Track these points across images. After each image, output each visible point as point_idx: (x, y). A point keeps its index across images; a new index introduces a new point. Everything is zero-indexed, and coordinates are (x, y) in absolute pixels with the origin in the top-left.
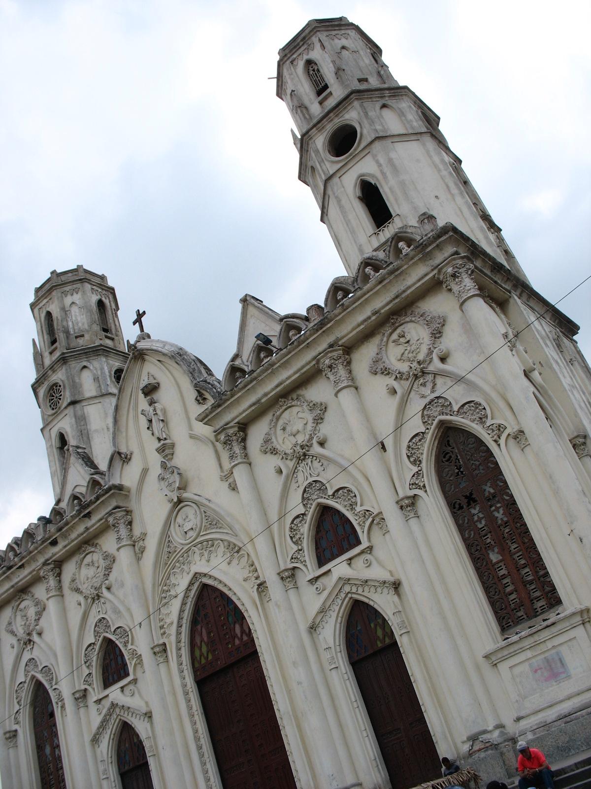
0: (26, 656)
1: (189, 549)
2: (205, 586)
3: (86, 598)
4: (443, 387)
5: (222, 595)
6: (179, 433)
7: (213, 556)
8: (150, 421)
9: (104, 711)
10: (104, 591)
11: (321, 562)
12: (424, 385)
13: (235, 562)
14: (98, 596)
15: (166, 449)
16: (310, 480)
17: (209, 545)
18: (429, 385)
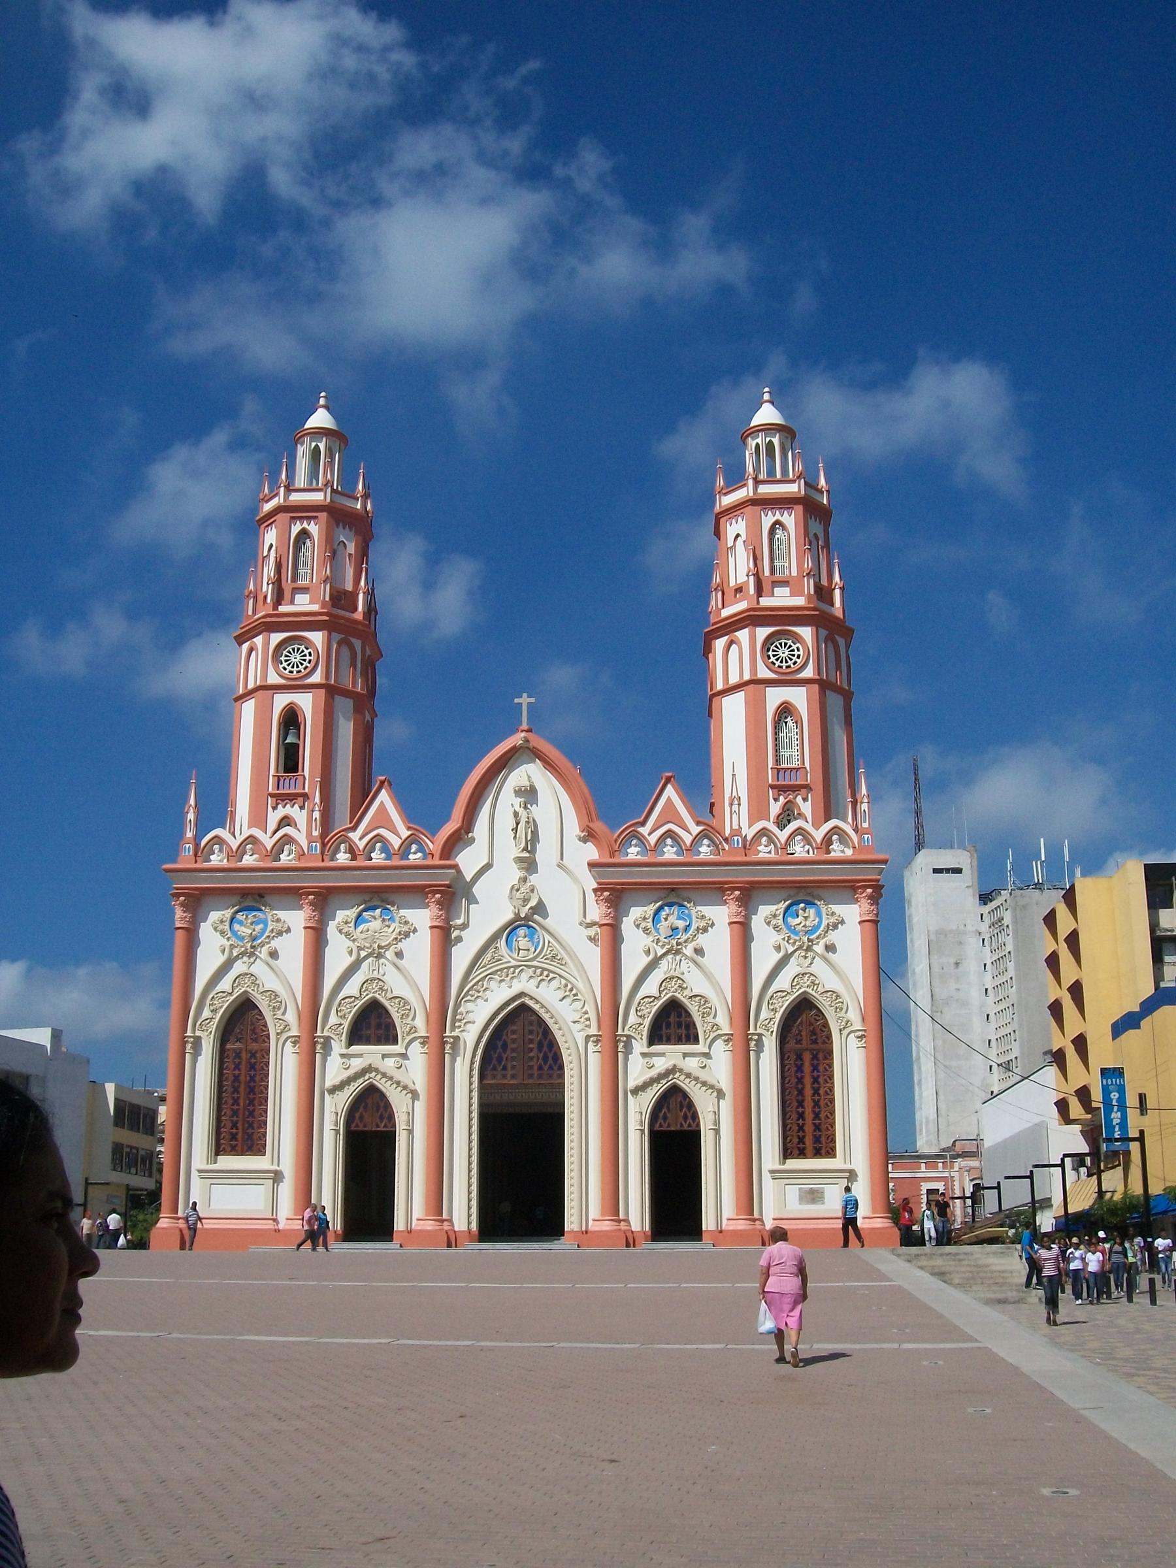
0: (239, 967)
1: (516, 967)
2: (523, 1008)
3: (360, 949)
4: (819, 967)
5: (541, 1022)
6: (546, 853)
7: (543, 983)
8: (517, 824)
9: (351, 1072)
10: (390, 954)
11: (651, 1043)
12: (806, 957)
13: (568, 1001)
14: (380, 956)
15: (529, 864)
16: (672, 973)
17: (544, 975)
18: (809, 961)
